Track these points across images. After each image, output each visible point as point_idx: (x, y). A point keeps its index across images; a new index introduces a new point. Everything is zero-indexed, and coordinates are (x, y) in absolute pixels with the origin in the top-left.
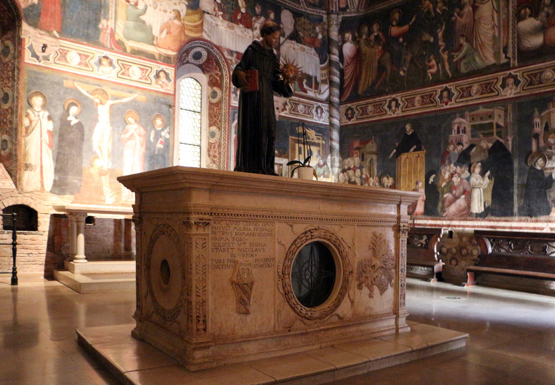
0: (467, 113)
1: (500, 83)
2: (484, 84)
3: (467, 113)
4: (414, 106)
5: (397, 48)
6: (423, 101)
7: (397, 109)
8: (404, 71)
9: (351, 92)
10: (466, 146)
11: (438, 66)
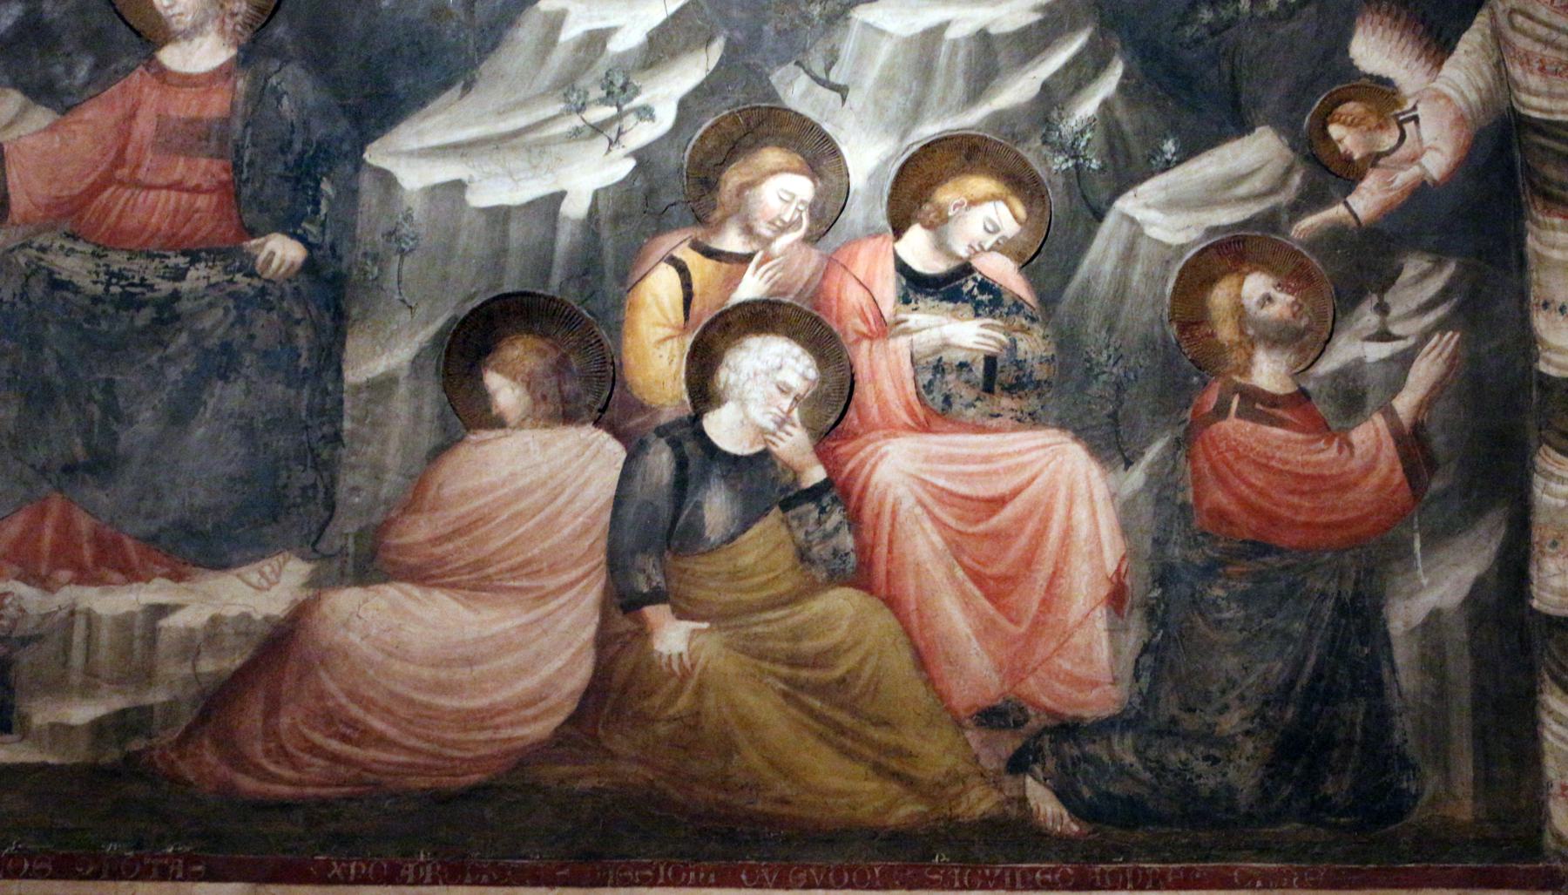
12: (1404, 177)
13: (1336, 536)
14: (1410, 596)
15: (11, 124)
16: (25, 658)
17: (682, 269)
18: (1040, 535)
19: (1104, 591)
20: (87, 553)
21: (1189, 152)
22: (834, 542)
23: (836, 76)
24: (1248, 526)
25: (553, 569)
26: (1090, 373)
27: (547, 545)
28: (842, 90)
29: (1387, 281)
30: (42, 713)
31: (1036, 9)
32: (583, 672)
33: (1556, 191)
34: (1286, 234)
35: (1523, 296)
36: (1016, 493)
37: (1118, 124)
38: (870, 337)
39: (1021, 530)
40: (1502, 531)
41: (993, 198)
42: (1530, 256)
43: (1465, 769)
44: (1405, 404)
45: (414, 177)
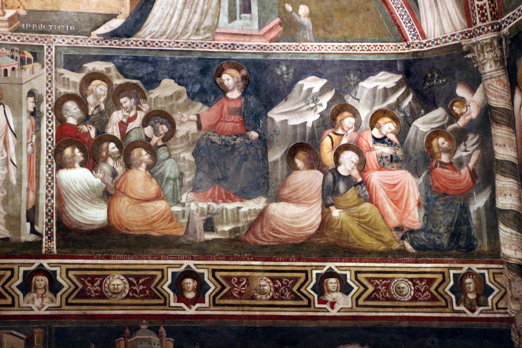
12: (468, 118)
13: (460, 192)
14: (474, 204)
15: (201, 109)
16: (215, 217)
17: (331, 137)
18: (404, 192)
19: (416, 203)
20: (224, 197)
21: (427, 112)
22: (364, 193)
23: (357, 97)
24: (443, 190)
25: (312, 199)
26: (411, 159)
27: (310, 194)
28: (358, 100)
29: (466, 139)
30: (220, 228)
31: (395, 83)
33: (498, 121)
34: (446, 129)
35: (491, 142)
36: (398, 183)
37: (412, 107)
38: (368, 151)
39: (400, 191)
40: (490, 191)
41: (390, 122)
42: (493, 134)
43: (486, 240)
44: (471, 165)
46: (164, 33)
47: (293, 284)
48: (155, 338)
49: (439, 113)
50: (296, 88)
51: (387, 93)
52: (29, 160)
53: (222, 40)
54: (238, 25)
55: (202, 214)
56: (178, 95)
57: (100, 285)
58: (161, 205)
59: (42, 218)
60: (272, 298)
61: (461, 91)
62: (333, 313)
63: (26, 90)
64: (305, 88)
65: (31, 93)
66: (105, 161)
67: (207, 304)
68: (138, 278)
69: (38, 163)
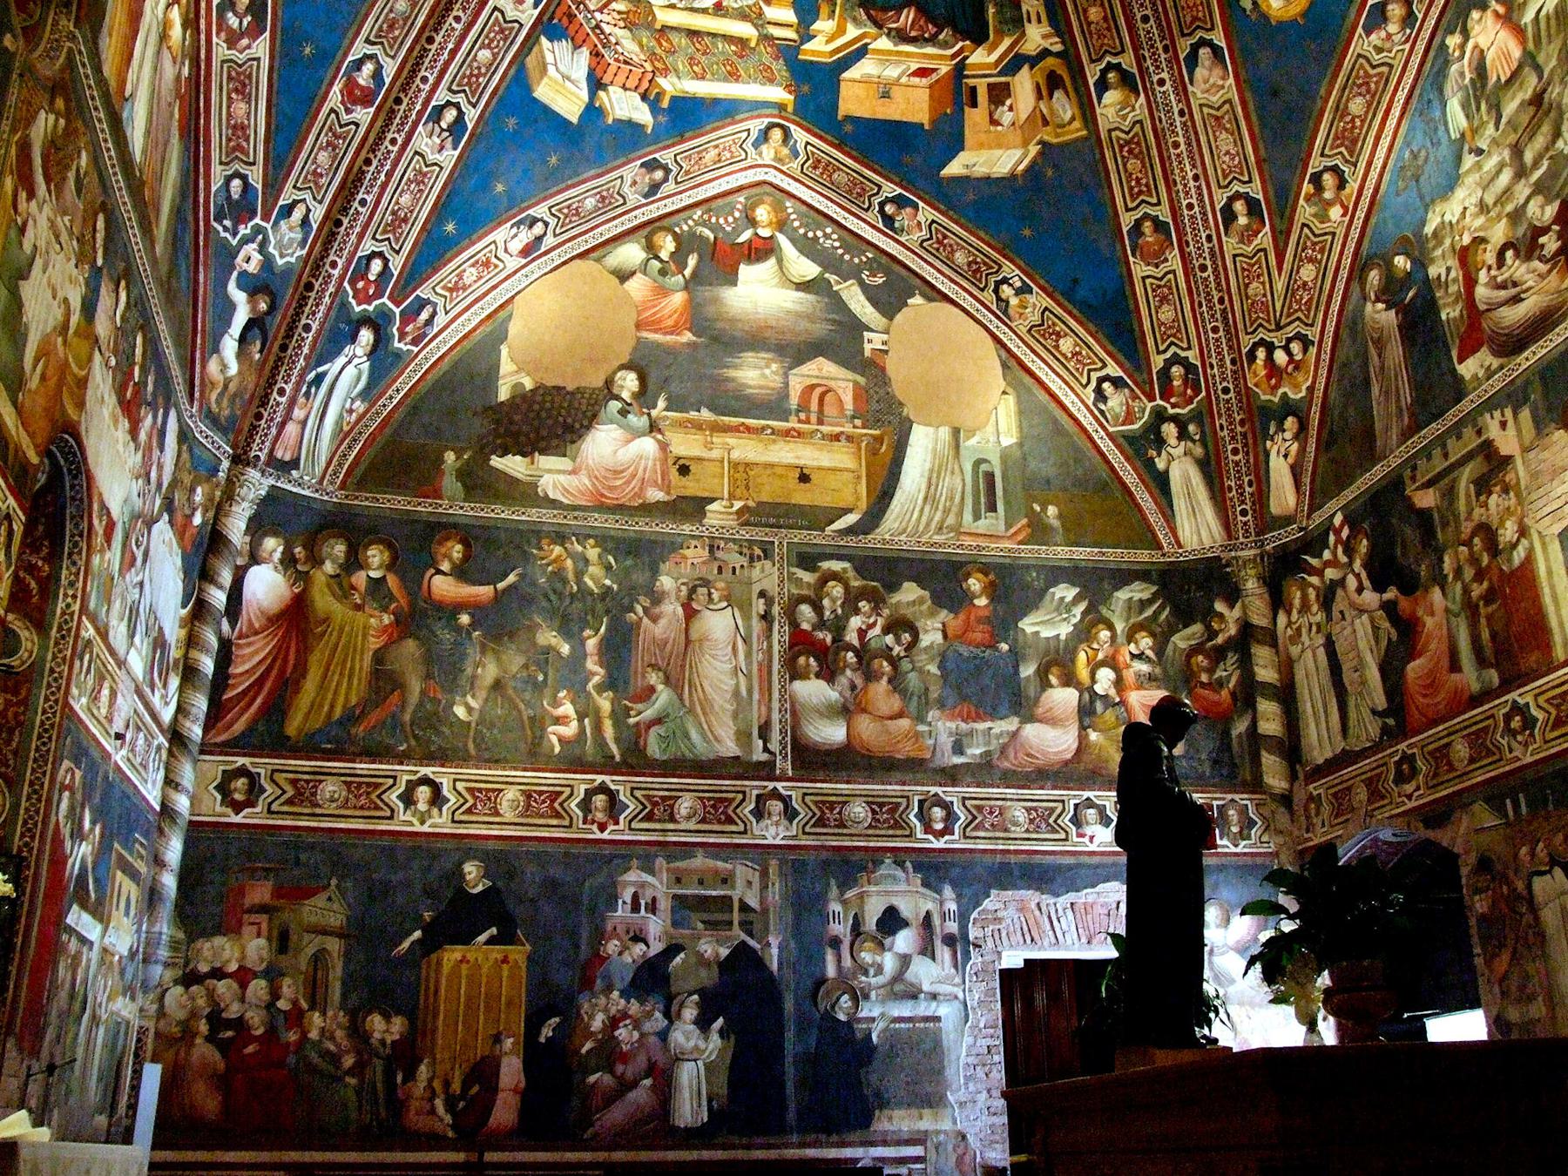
0: (660, 862)
1: (752, 806)
2: (709, 799)
3: (660, 862)
4: (497, 814)
5: (446, 636)
6: (529, 805)
7: (435, 811)
8: (470, 710)
9: (255, 720)
10: (656, 947)
11: (581, 720)
21: (1185, 626)
29: (1224, 658)
30: (969, 751)
32: (1075, 745)
44: (1231, 685)
45: (1029, 630)
46: (904, 531)
47: (1050, 815)
48: (900, 873)
49: (1197, 628)
50: (1048, 597)
51: (1144, 604)
52: (760, 670)
53: (968, 541)
54: (983, 525)
55: (951, 734)
56: (921, 601)
57: (840, 813)
58: (904, 723)
59: (775, 736)
60: (1027, 831)
61: (1219, 606)
62: (1093, 848)
63: (756, 589)
64: (1057, 596)
65: (762, 594)
66: (843, 672)
67: (956, 837)
68: (881, 805)
69: (770, 673)
